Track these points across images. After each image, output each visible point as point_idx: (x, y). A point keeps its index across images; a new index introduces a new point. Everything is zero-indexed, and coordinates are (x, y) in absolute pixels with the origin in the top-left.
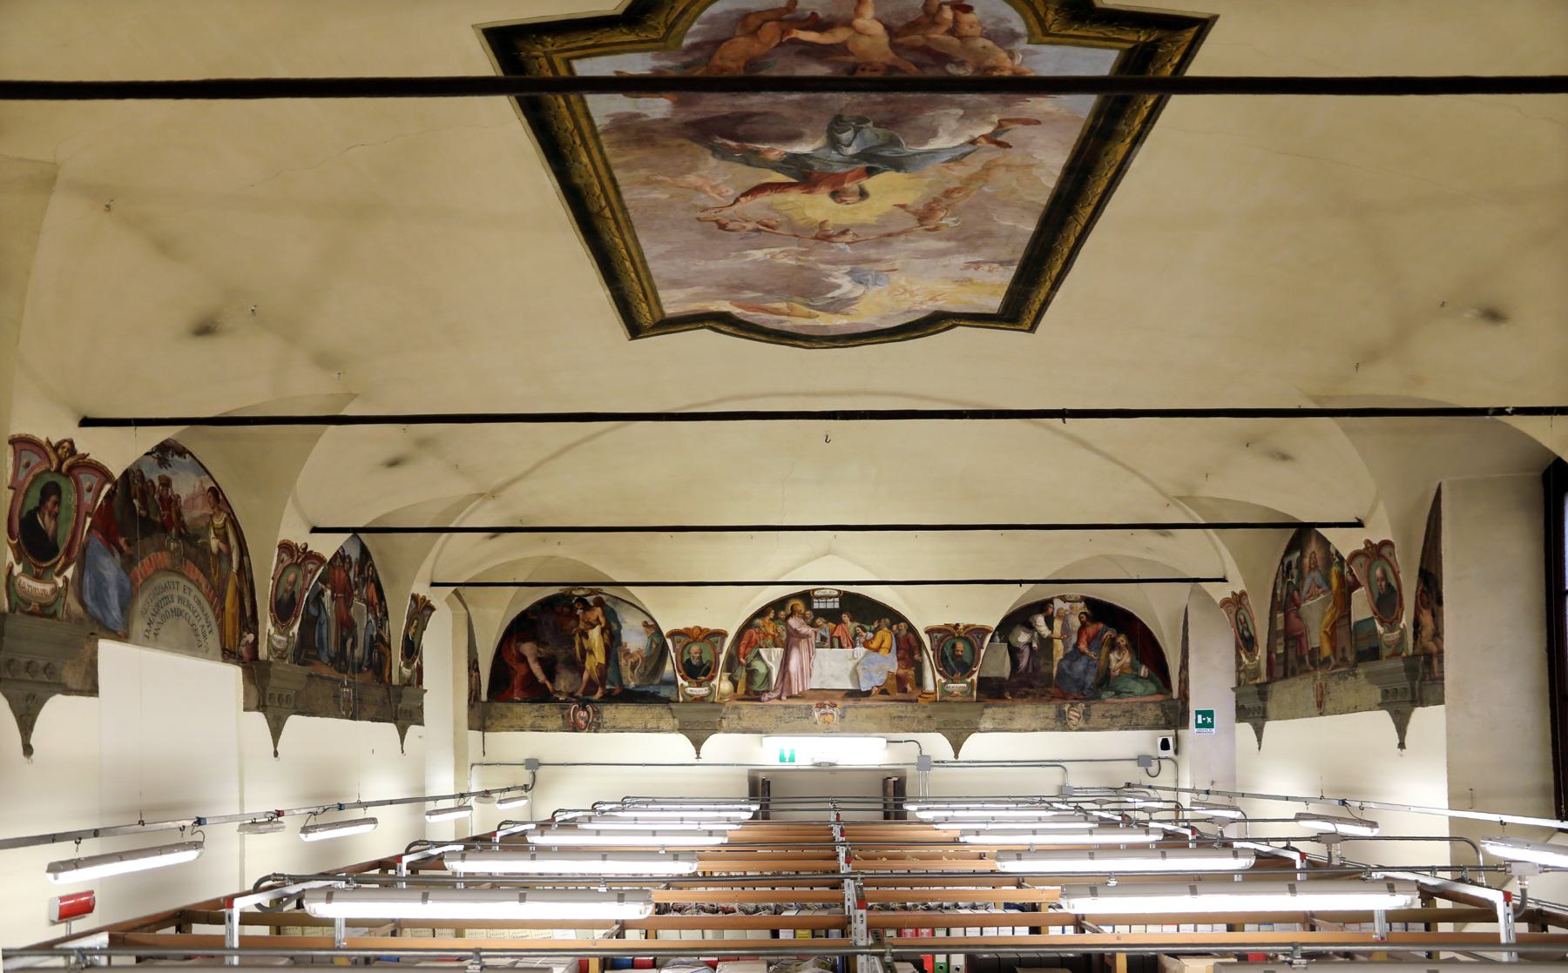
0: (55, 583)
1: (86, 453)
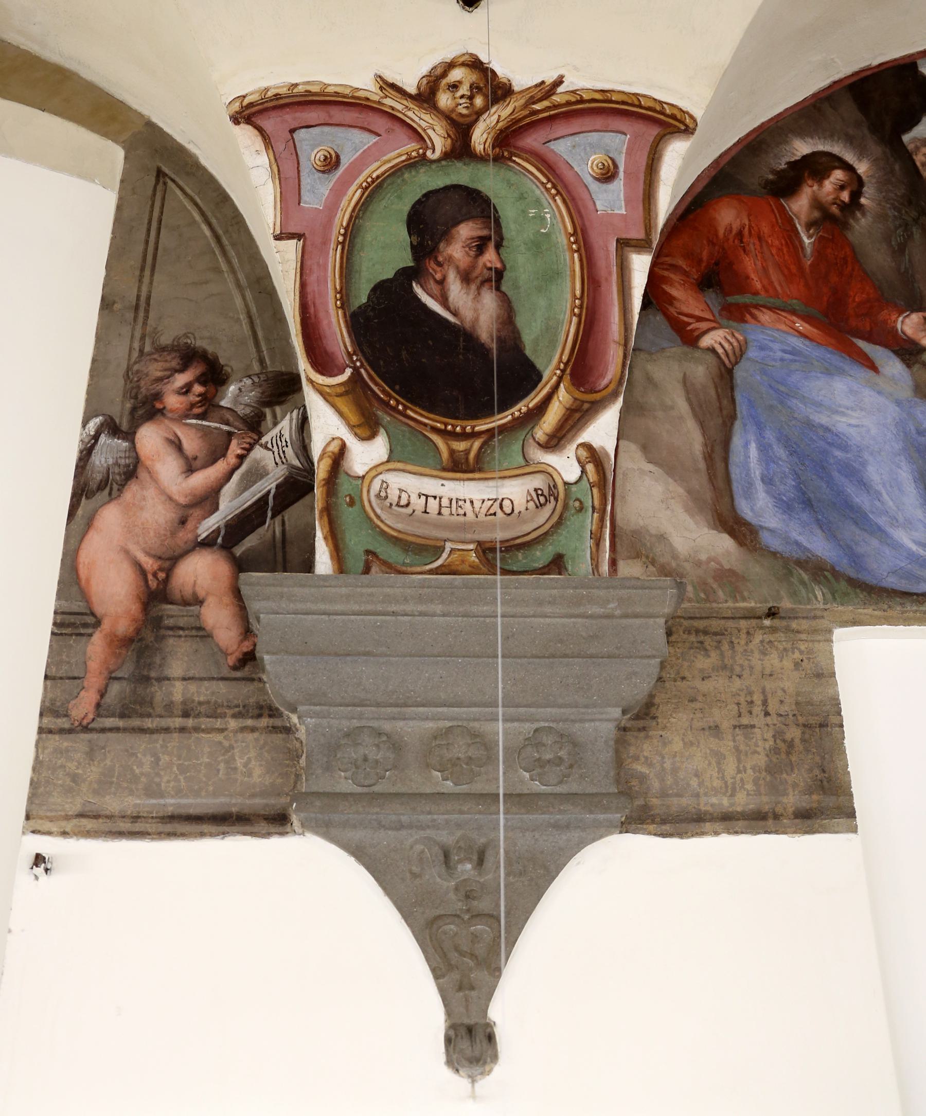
0: (546, 471)
1: (550, 78)
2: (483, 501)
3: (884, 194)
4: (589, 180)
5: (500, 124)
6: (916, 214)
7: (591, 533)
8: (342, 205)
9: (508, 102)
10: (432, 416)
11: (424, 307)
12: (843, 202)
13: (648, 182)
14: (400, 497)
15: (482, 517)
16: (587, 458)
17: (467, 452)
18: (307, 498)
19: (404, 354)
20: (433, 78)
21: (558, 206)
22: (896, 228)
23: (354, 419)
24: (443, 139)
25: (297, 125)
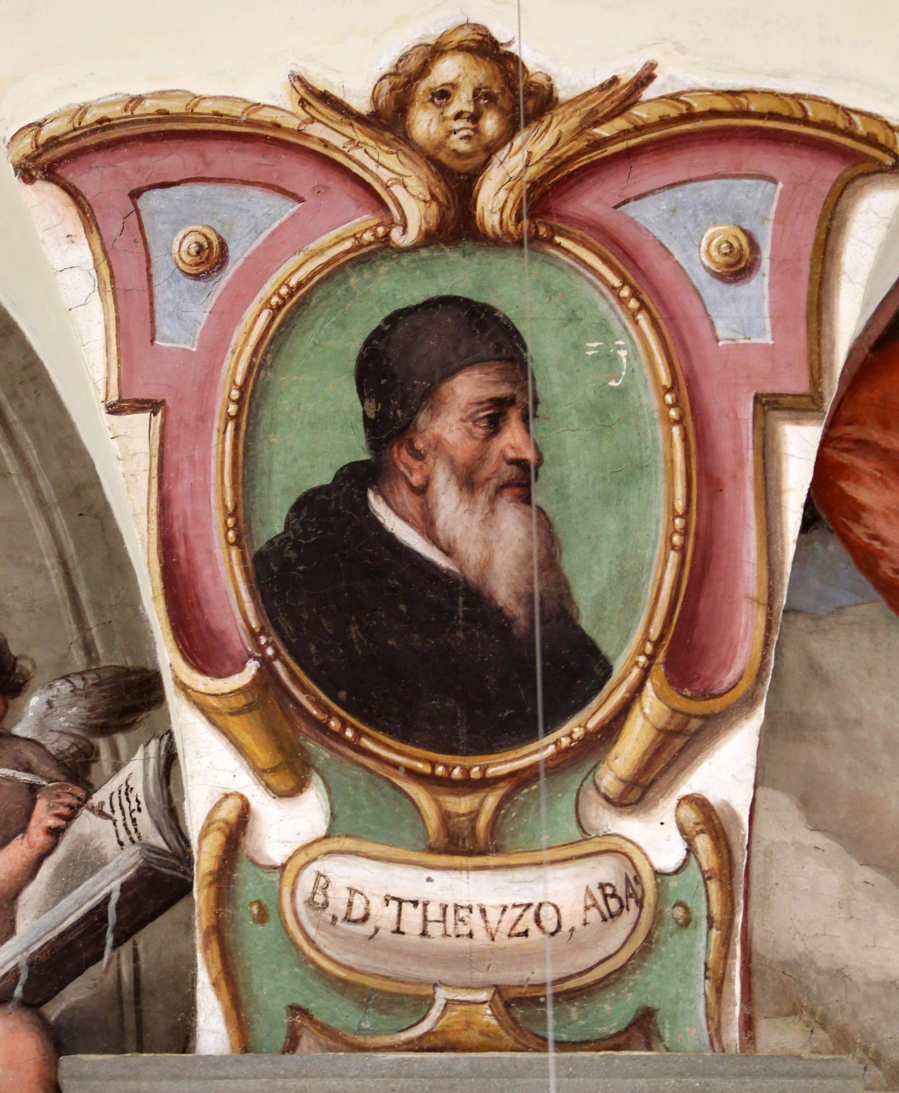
1: (628, 71)
2: (505, 909)
4: (701, 278)
5: (532, 170)
7: (707, 969)
8: (232, 343)
9: (546, 123)
10: (407, 748)
11: (390, 540)
13: (817, 277)
14: (350, 904)
15: (502, 939)
16: (697, 824)
17: (474, 816)
18: (179, 908)
19: (354, 630)
20: (402, 79)
21: (641, 334)
23: (265, 757)
24: (422, 204)
25: (144, 184)
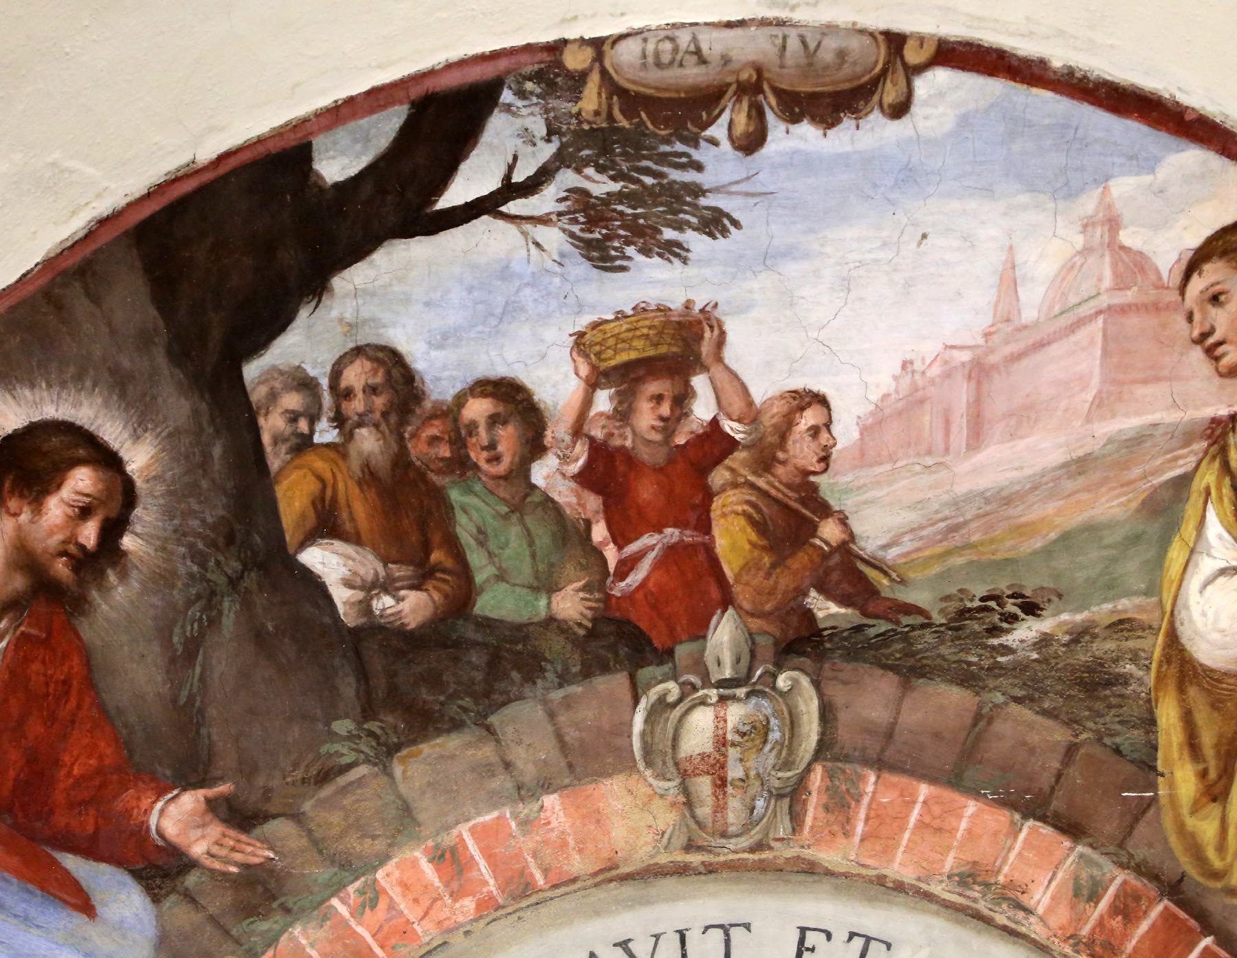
3: (176, 522)
6: (237, 565)
12: (82, 547)
22: (189, 603)
